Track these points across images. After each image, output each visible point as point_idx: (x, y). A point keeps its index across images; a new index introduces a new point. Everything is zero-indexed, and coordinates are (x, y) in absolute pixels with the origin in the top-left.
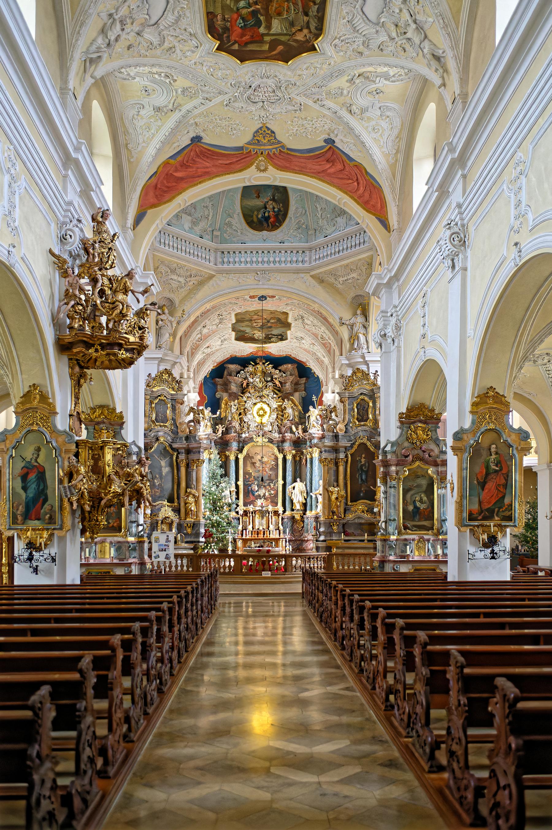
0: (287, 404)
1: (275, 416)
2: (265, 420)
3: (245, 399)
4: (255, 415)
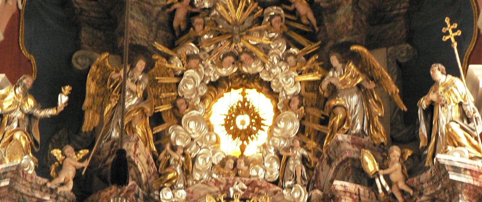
0: (343, 74)
1: (292, 127)
2: (253, 149)
3: (177, 64)
4: (220, 130)
